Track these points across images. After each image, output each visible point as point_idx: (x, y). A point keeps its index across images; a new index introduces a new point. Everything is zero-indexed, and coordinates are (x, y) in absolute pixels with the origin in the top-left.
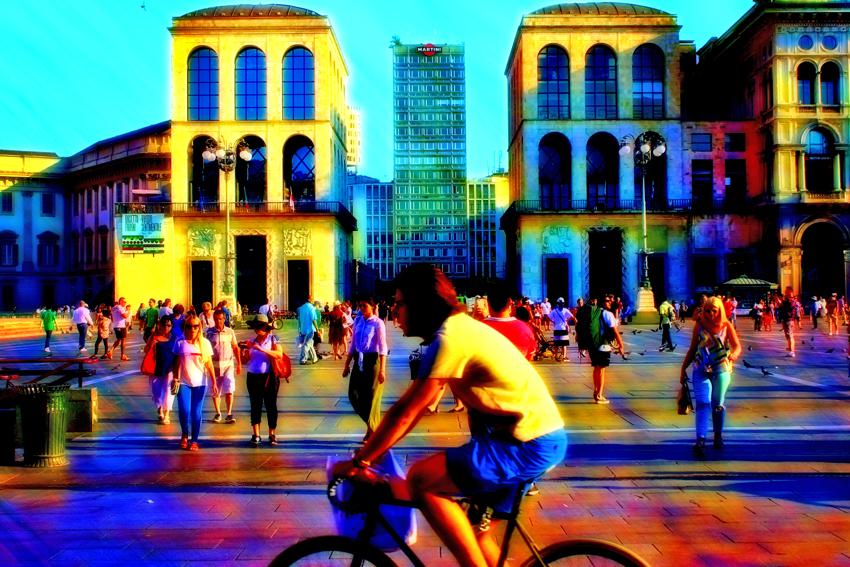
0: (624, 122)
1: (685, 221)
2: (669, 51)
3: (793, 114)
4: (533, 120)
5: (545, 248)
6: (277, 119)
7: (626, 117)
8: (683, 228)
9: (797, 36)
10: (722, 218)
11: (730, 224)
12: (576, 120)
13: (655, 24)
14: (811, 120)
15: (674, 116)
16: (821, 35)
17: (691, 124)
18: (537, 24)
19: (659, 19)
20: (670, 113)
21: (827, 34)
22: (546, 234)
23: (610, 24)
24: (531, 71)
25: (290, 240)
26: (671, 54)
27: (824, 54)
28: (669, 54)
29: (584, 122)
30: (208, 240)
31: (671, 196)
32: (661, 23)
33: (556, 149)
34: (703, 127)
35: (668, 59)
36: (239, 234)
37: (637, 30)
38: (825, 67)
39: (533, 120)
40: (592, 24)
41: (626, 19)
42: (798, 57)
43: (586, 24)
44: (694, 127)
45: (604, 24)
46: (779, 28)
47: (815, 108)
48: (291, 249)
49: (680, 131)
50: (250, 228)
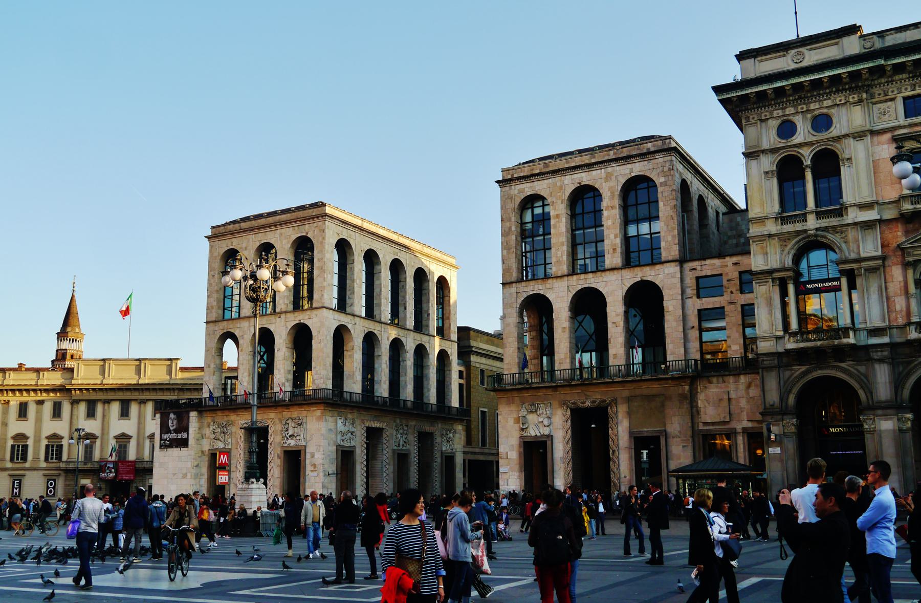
0: (611, 273)
1: (687, 388)
2: (662, 180)
3: (772, 227)
4: (512, 283)
5: (522, 429)
6: (284, 310)
7: (613, 266)
8: (683, 397)
9: (774, 124)
10: (737, 381)
11: (749, 386)
12: (557, 277)
13: (645, 151)
14: (799, 233)
15: (670, 258)
16: (809, 116)
17: (696, 264)
18: (515, 176)
19: (650, 145)
20: (665, 255)
21: (817, 112)
22: (523, 412)
23: (593, 161)
24: (510, 228)
26: (664, 184)
27: (814, 139)
28: (661, 184)
29: (566, 278)
31: (669, 357)
32: (652, 149)
33: (538, 308)
34: (710, 266)
35: (660, 189)
37: (622, 162)
38: (816, 158)
39: (512, 283)
40: (573, 164)
41: (612, 152)
42: (773, 151)
43: (567, 166)
44: (699, 268)
45: (587, 162)
46: (747, 118)
47: (805, 215)
49: (678, 275)
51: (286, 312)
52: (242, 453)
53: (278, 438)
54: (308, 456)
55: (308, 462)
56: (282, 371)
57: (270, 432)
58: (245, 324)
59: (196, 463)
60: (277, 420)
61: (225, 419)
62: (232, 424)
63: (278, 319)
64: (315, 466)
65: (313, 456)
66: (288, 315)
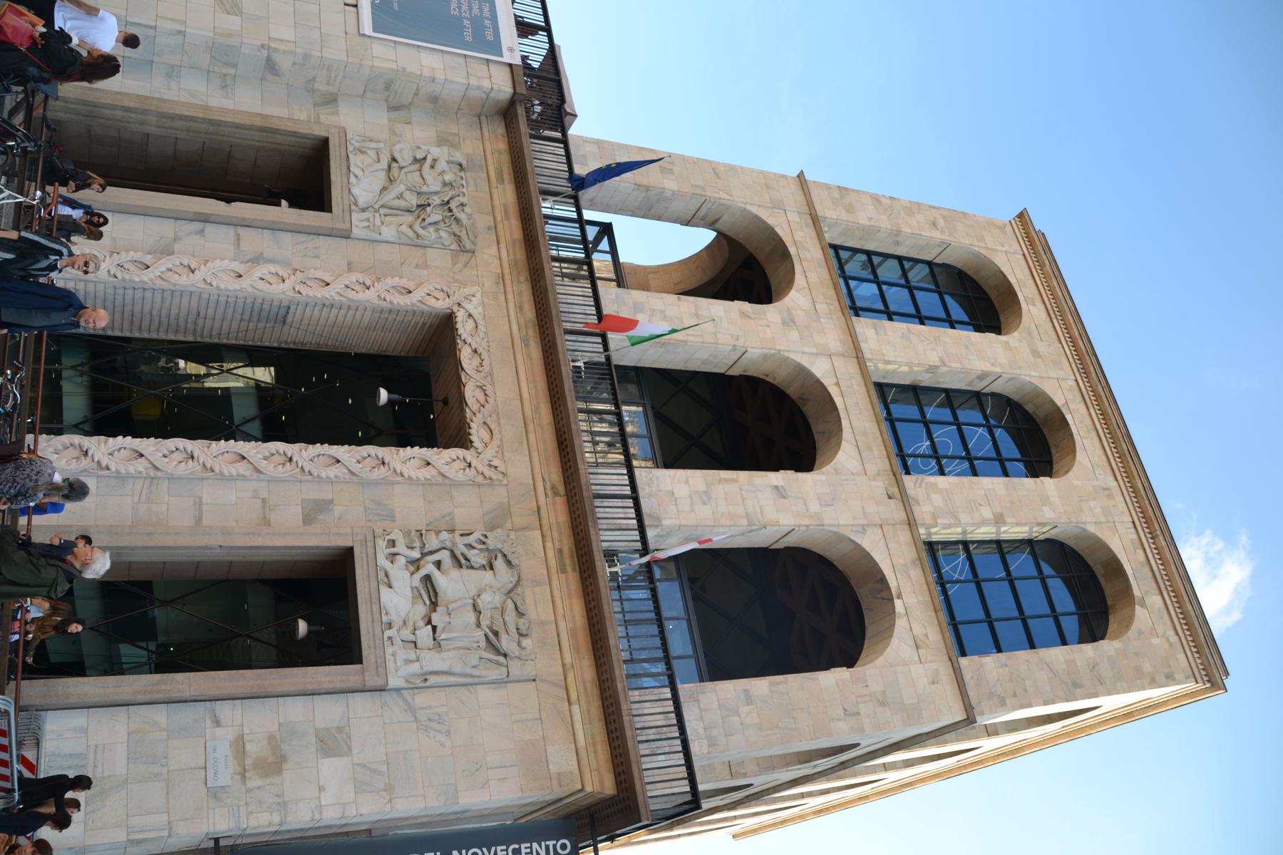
25: (460, 562)
30: (434, 210)
36: (464, 328)
48: (415, 564)
50: (497, 376)
51: (911, 523)
52: (329, 294)
53: (410, 508)
54: (327, 711)
55: (294, 710)
56: (704, 514)
57: (443, 457)
58: (830, 332)
59: (284, 63)
60: (496, 497)
61: (484, 221)
62: (463, 249)
63: (880, 486)
64: (274, 765)
65: (332, 743)
66: (904, 536)
